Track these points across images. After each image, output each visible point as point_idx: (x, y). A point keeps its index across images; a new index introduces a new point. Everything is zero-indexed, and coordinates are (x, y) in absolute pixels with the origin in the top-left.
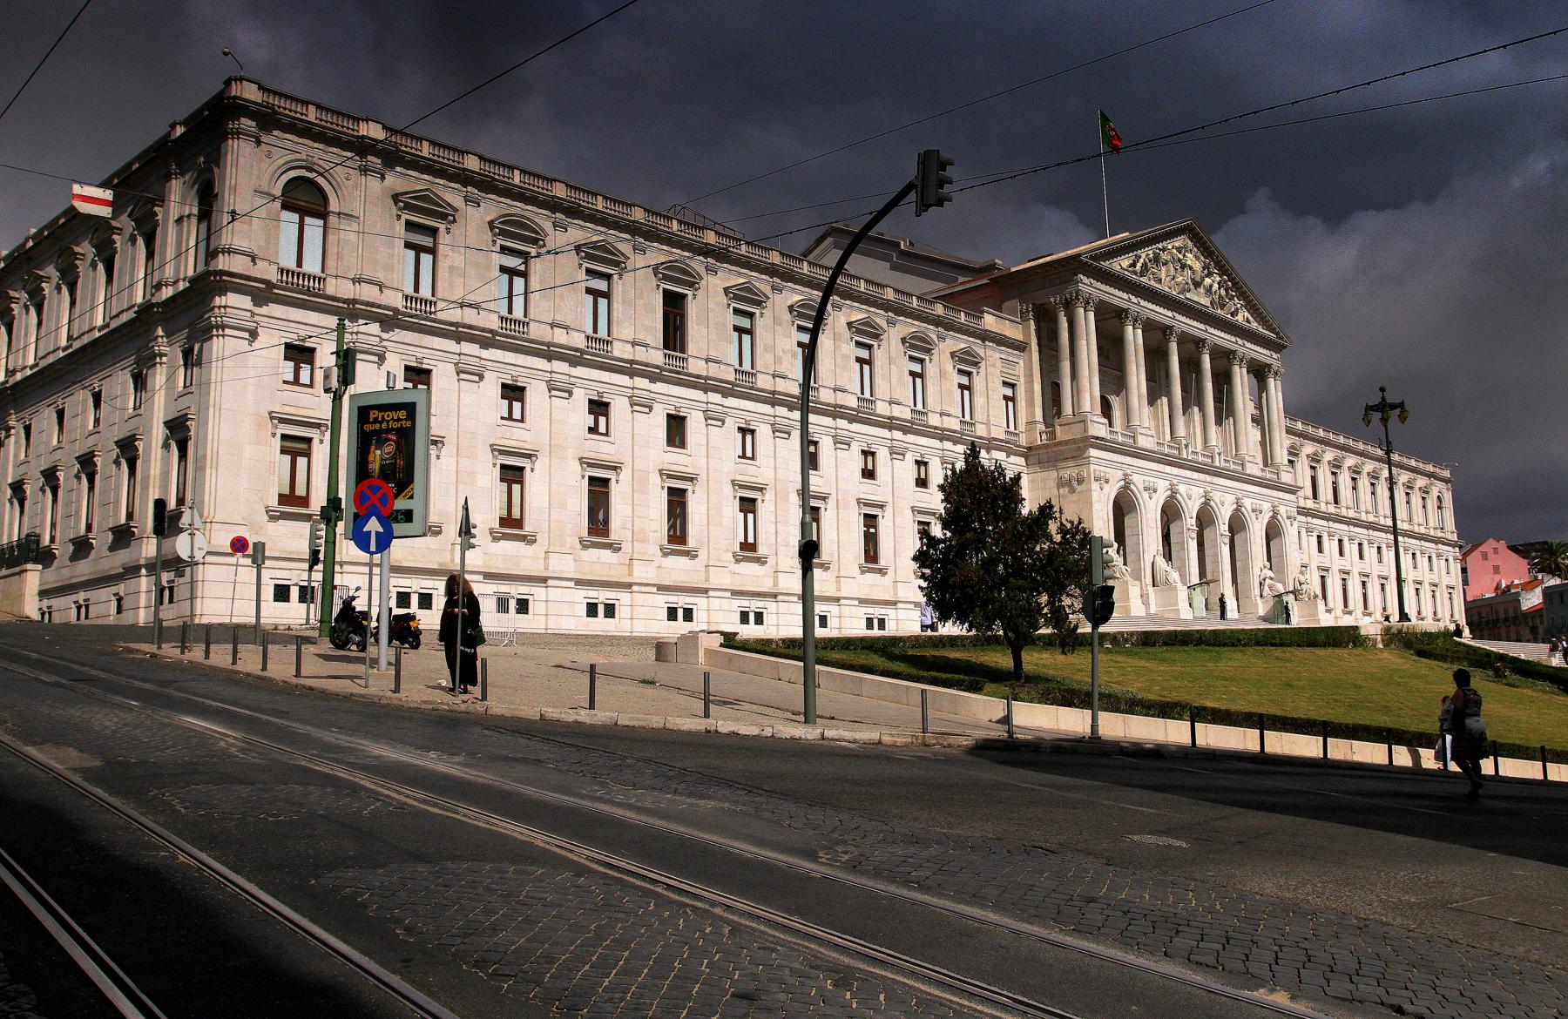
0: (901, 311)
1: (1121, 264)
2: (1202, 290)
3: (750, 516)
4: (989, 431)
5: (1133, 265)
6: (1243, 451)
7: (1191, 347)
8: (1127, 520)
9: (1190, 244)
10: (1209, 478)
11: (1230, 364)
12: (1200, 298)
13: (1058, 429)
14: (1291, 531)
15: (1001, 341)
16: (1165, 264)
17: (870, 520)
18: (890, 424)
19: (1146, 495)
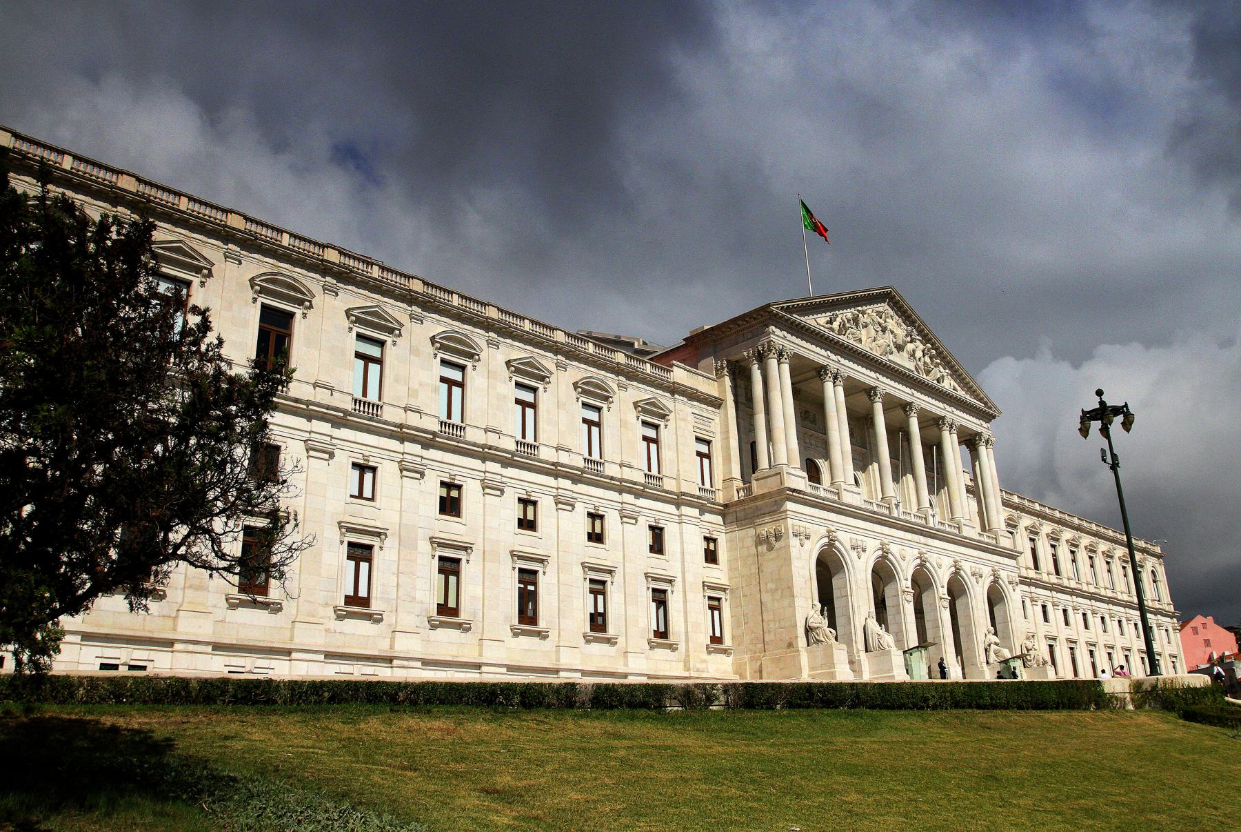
0: (572, 355)
1: (818, 321)
2: (905, 354)
3: (364, 566)
4: (679, 486)
5: (830, 322)
6: (958, 514)
7: (899, 408)
8: (836, 582)
9: (891, 312)
10: (923, 539)
11: (941, 430)
12: (901, 360)
13: (754, 483)
14: (1014, 596)
15: (693, 396)
16: (866, 326)
17: (528, 577)
18: (555, 471)
19: (854, 554)
